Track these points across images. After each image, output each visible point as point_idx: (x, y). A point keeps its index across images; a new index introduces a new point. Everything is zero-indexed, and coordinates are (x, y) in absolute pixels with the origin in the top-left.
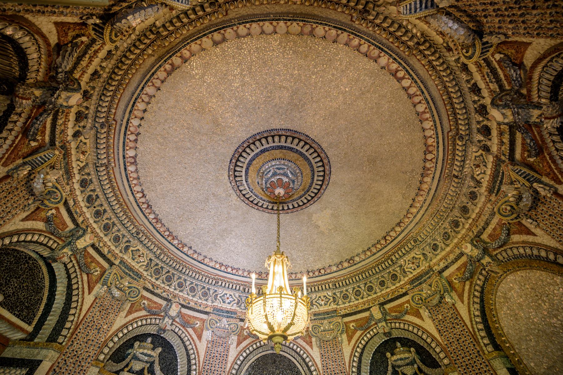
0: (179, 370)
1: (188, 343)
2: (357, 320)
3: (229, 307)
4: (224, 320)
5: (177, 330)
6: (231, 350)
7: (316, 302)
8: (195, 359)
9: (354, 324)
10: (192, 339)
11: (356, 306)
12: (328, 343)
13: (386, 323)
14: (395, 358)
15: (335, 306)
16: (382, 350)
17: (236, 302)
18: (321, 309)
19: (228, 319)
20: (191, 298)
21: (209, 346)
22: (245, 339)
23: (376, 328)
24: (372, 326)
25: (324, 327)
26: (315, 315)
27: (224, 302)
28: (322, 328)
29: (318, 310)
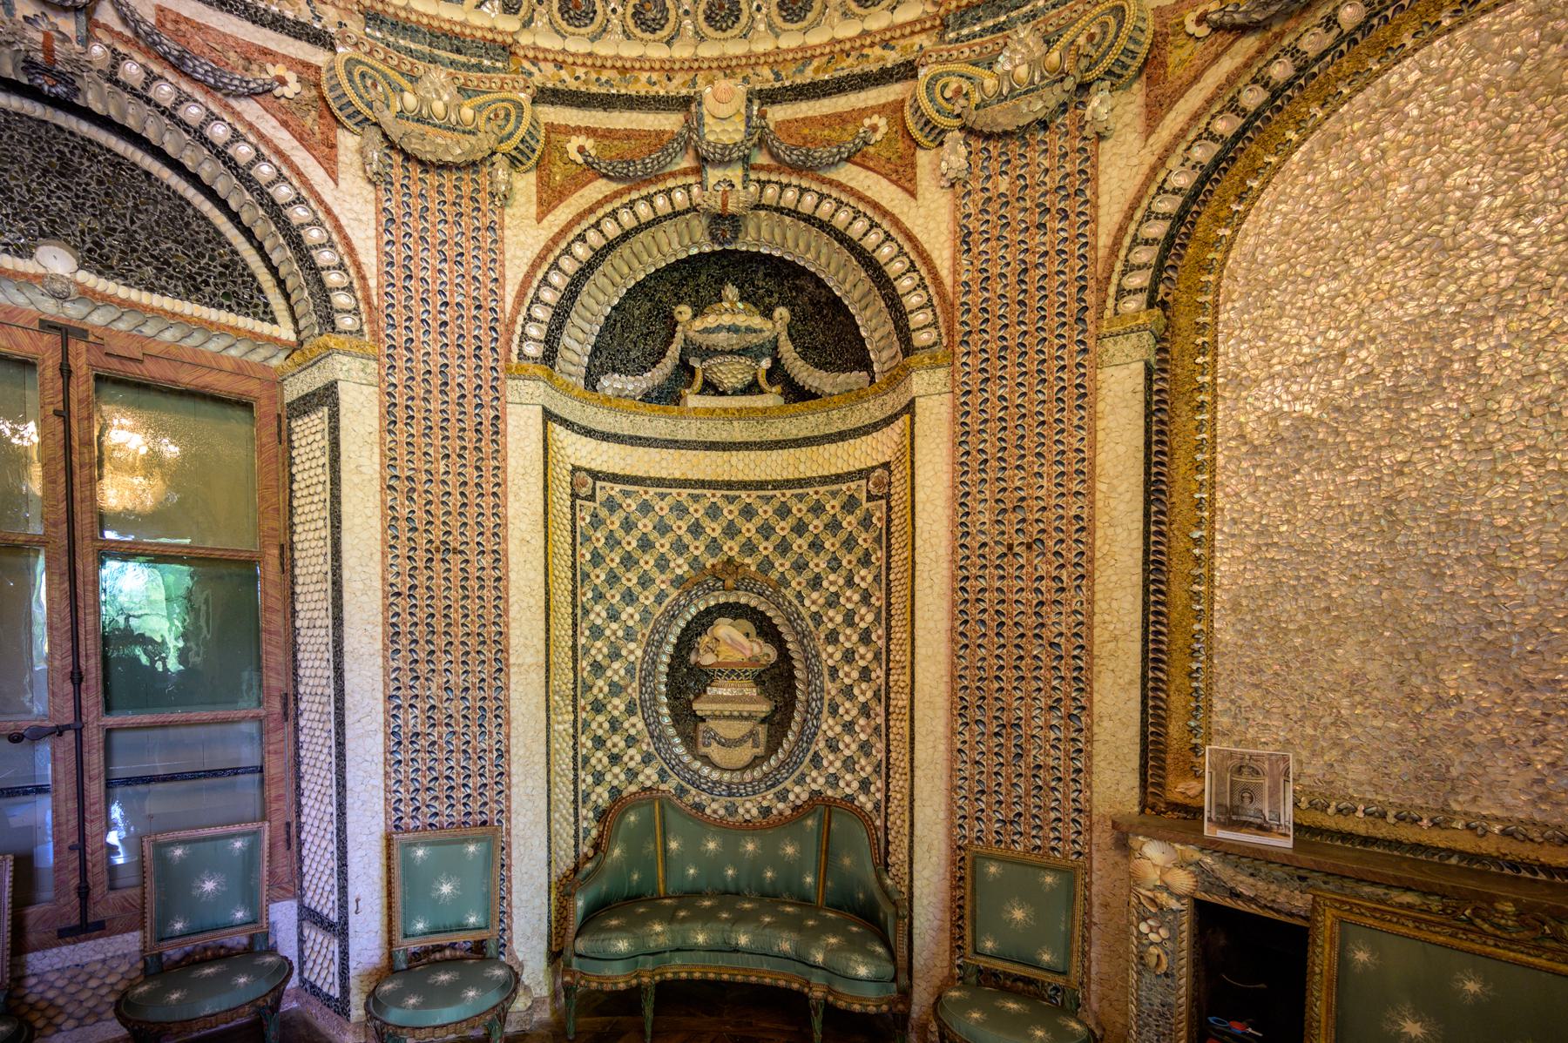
9: (589, 144)
11: (623, 70)
13: (746, 180)
14: (698, 324)
16: (664, 293)
23: (687, 187)
24: (673, 175)
25: (422, 101)
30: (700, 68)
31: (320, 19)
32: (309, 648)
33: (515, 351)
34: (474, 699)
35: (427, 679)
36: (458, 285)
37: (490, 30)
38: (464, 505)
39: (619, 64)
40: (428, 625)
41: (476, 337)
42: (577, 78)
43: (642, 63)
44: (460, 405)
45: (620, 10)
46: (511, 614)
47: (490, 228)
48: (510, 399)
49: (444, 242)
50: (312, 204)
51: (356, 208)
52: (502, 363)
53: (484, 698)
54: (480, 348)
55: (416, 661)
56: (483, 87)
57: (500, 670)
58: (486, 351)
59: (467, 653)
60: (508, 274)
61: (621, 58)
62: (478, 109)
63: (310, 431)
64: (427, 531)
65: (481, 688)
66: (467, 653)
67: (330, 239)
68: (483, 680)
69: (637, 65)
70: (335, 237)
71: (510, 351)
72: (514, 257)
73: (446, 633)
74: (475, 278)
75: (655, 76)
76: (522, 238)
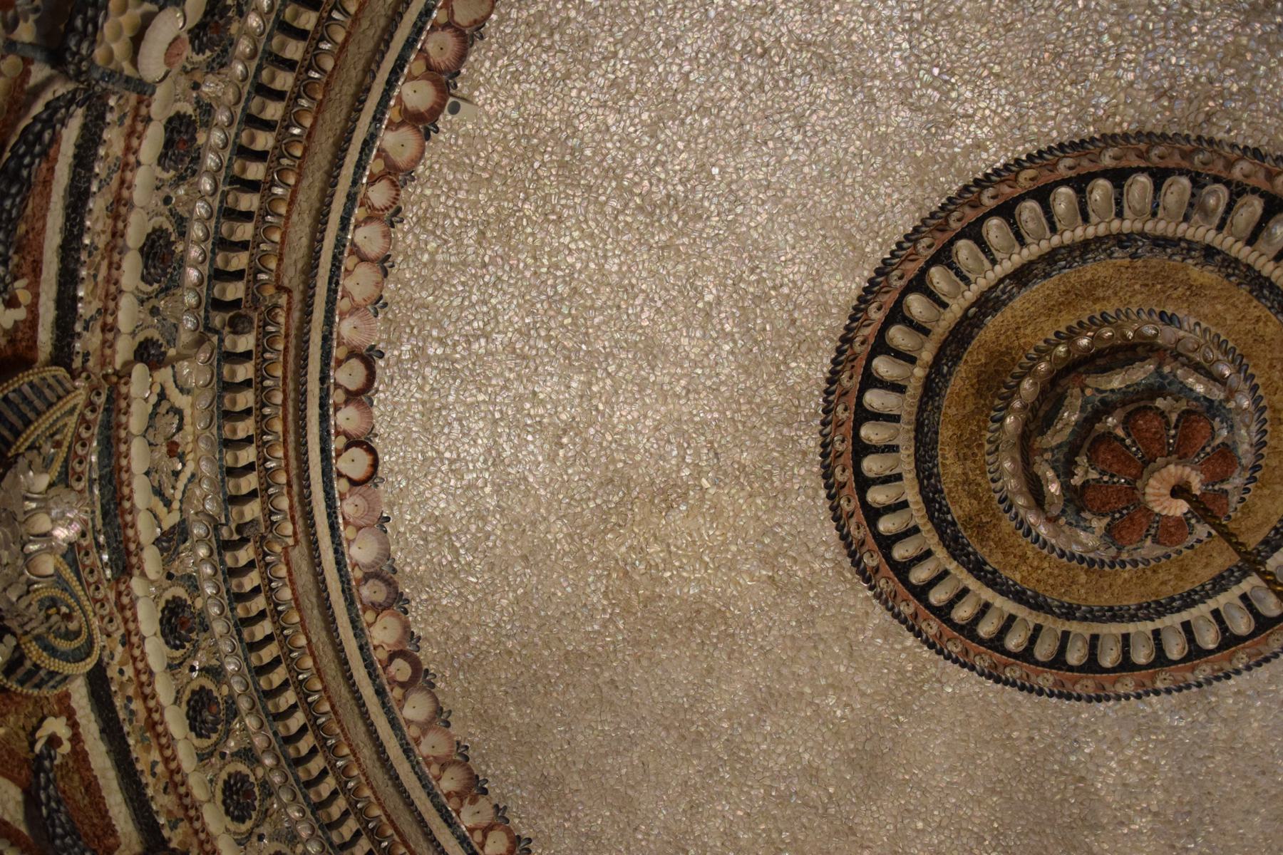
2: (79, 755)
11: (152, 725)
30: (191, 820)
39: (156, 717)
42: (121, 672)
43: (166, 744)
45: (195, 674)
56: (85, 574)
61: (162, 715)
69: (164, 741)
75: (160, 768)
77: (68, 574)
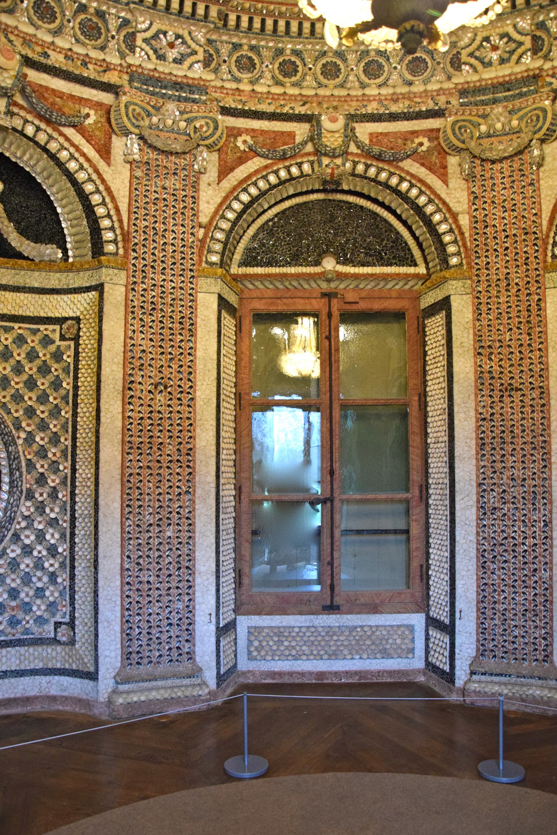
0: (66, 231)
1: (72, 166)
3: (179, 71)
4: (171, 107)
5: (30, 130)
6: (203, 186)
7: (471, 55)
8: (104, 203)
10: (84, 155)
12: (498, 166)
15: (539, 63)
17: (200, 56)
18: (486, 76)
19: (182, 106)
20: (48, 38)
21: (139, 173)
22: (242, 160)
25: (490, 127)
26: (463, 93)
27: (161, 57)
28: (483, 128)
29: (475, 78)
31: (437, 104)
32: (435, 455)
33: (550, 254)
34: (529, 486)
35: (501, 473)
36: (514, 223)
37: (526, 71)
38: (521, 359)
40: (501, 438)
41: (525, 252)
44: (517, 296)
46: (552, 428)
47: (531, 184)
48: (547, 286)
49: (505, 201)
50: (436, 201)
51: (458, 196)
52: (541, 265)
53: (535, 486)
54: (528, 258)
55: (494, 461)
56: (523, 106)
57: (545, 467)
58: (532, 259)
59: (524, 456)
60: (544, 207)
62: (520, 119)
63: (435, 325)
64: (500, 378)
65: (533, 479)
66: (524, 456)
67: (445, 217)
68: (534, 473)
70: (448, 215)
71: (546, 255)
72: (547, 196)
73: (512, 443)
74: (523, 217)
76: (551, 183)
77: (522, 113)
